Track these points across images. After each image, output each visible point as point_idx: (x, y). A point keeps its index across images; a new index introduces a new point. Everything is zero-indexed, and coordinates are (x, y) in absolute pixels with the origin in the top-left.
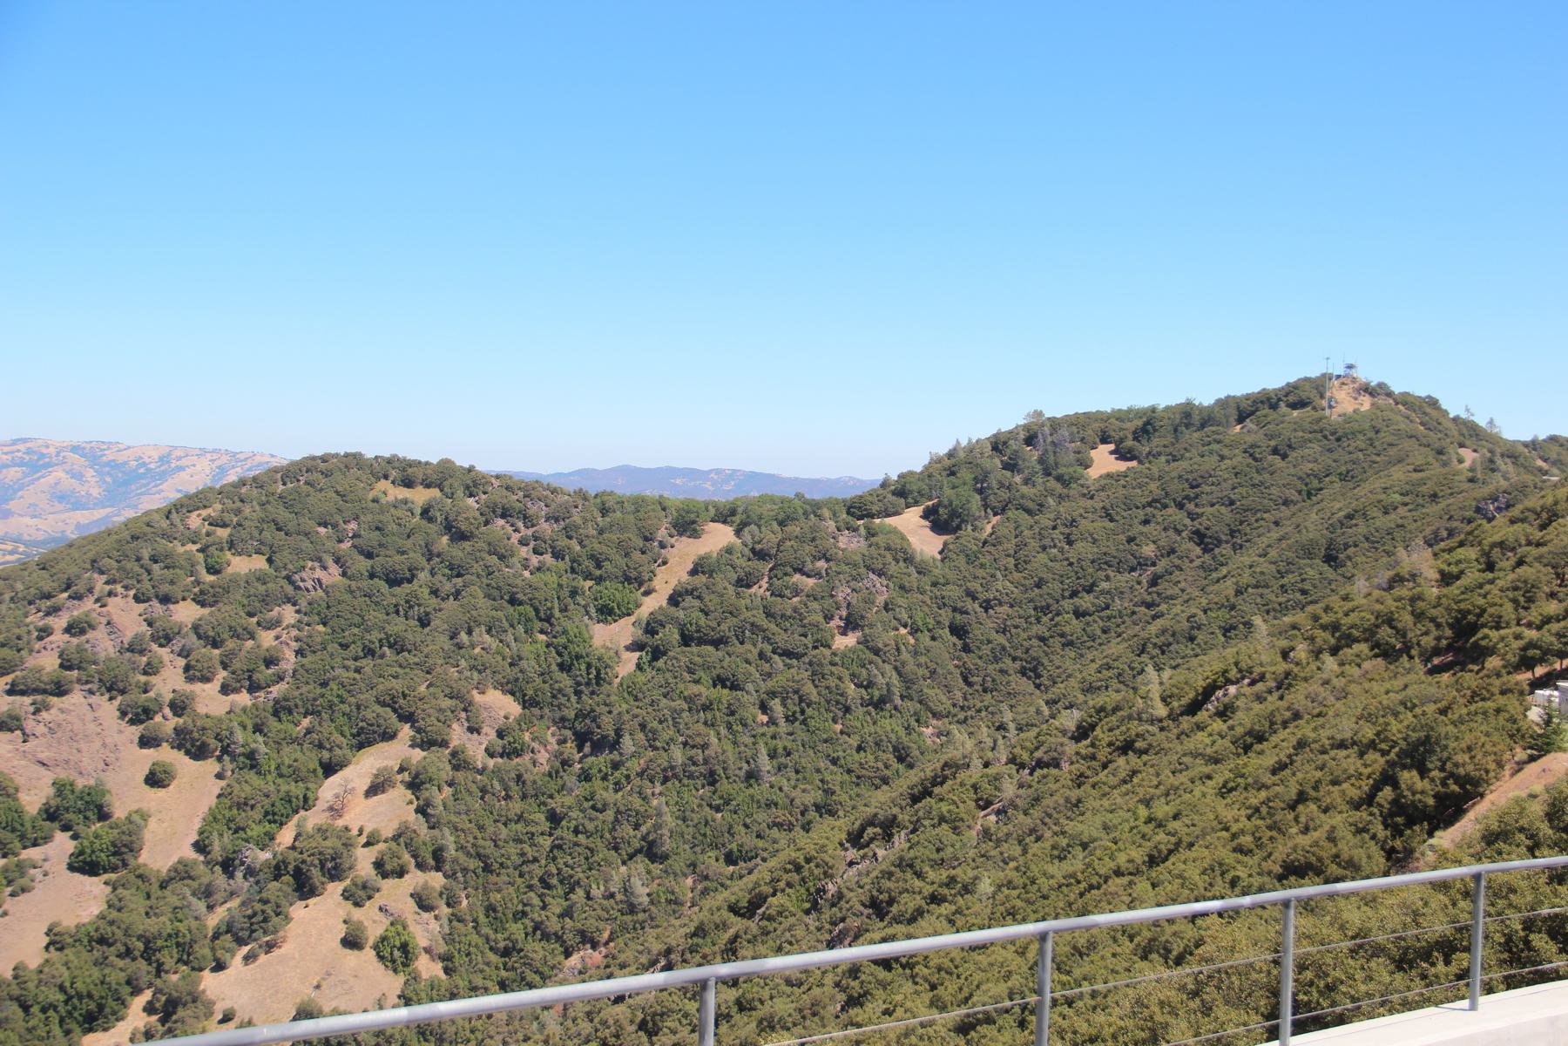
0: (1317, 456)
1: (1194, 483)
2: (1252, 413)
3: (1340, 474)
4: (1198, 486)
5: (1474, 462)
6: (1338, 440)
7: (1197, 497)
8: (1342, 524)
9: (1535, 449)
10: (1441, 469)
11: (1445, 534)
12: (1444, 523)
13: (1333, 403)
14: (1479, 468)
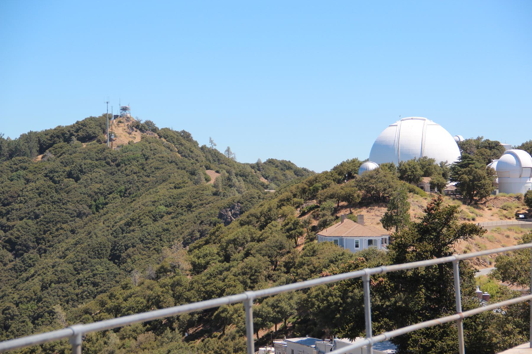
0: (103, 178)
1: (6, 202)
2: (51, 145)
3: (120, 192)
4: (8, 204)
5: (217, 180)
6: (118, 165)
7: (8, 213)
8: (123, 231)
9: (259, 170)
10: (194, 186)
11: (198, 235)
12: (197, 227)
13: (113, 137)
14: (220, 185)
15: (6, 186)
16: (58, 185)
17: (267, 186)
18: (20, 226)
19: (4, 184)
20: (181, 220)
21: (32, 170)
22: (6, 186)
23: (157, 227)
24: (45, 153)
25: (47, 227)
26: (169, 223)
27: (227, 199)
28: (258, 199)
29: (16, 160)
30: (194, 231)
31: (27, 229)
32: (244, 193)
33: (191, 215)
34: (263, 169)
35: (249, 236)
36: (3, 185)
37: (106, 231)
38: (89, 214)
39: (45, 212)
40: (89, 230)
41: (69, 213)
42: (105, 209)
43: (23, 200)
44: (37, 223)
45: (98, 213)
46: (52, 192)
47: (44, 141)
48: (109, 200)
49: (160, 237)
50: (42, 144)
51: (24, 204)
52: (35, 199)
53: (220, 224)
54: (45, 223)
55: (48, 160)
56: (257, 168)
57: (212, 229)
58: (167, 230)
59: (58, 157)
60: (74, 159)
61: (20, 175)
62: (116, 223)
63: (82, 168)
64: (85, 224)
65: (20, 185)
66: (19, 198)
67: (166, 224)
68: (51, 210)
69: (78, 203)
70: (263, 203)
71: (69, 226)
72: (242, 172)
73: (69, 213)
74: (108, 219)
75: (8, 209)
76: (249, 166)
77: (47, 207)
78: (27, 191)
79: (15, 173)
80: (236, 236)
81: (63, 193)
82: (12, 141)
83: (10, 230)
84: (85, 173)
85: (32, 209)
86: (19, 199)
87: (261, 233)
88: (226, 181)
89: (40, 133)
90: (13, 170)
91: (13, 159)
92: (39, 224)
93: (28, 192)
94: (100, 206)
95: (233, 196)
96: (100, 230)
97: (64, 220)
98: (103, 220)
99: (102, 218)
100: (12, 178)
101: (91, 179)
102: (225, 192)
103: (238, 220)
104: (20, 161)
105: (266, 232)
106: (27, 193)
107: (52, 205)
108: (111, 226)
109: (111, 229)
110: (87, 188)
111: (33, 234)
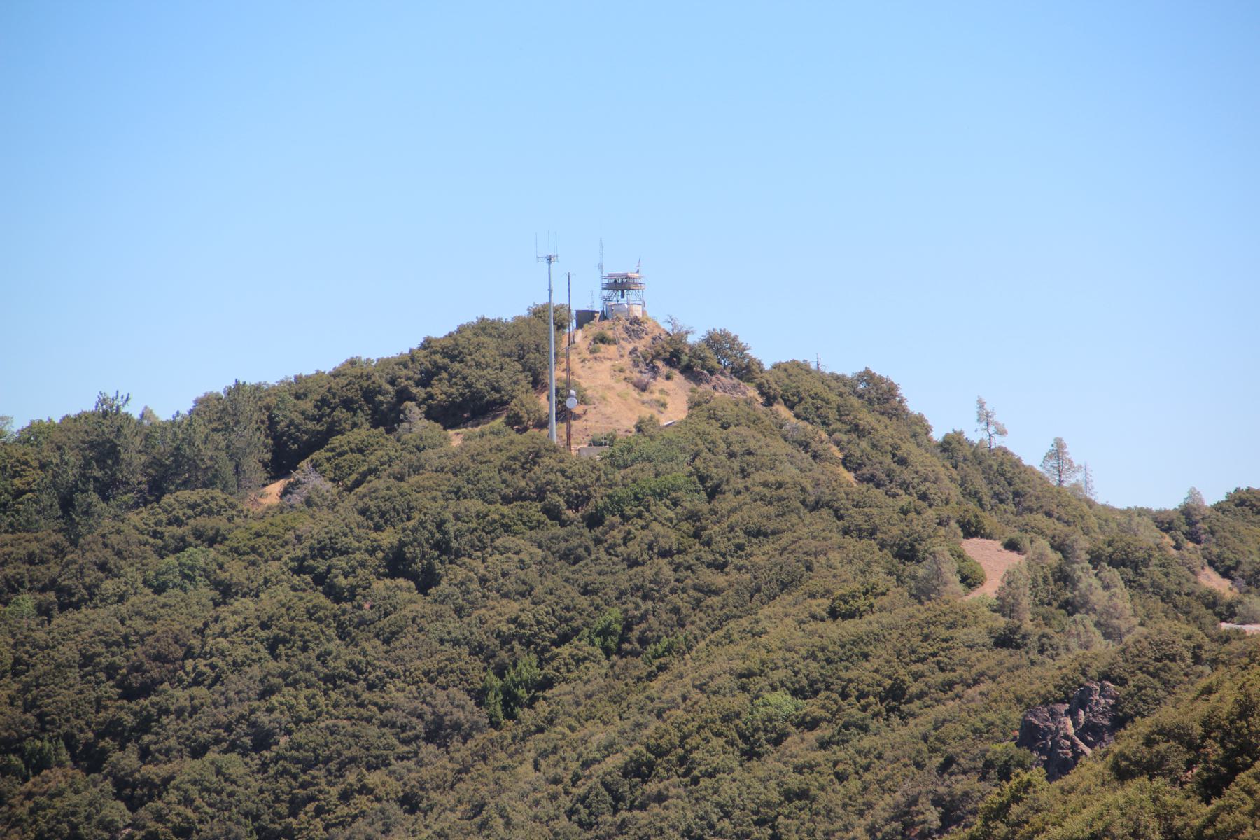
0: (532, 574)
1: (136, 680)
2: (319, 441)
3: (605, 632)
4: (147, 689)
5: (1010, 581)
6: (594, 521)
7: (145, 724)
8: (618, 798)
9: (1194, 537)
10: (912, 609)
11: (933, 816)
12: (926, 783)
13: (571, 403)
14: (1026, 602)
15: (139, 613)
16: (347, 606)
17: (1230, 606)
18: (194, 783)
19: (128, 604)
20: (859, 752)
21: (244, 545)
22: (139, 613)
23: (757, 785)
24: (296, 475)
25: (304, 786)
26: (811, 768)
27: (1058, 664)
28: (1189, 661)
29: (176, 505)
30: (914, 801)
31: (224, 796)
32: (1128, 639)
33: (904, 731)
34: (1213, 532)
35: (1154, 823)
36: (123, 609)
37: (544, 802)
38: (475, 727)
39: (298, 721)
40: (478, 796)
41: (393, 725)
42: (541, 706)
43: (207, 670)
44: (264, 767)
45: (511, 723)
46: (323, 638)
47: (292, 422)
48: (557, 670)
49: (773, 828)
50: (283, 434)
51: (210, 687)
52: (256, 667)
53: (1026, 770)
54: (294, 769)
55: (309, 502)
56: (1185, 528)
57: (993, 794)
58: (803, 794)
59: (350, 490)
60: (415, 495)
61: (192, 568)
62: (586, 765)
63: (446, 533)
64: (459, 772)
65: (195, 608)
66: (189, 664)
67: (798, 770)
68: (319, 714)
69: (431, 681)
70: (1213, 679)
71: (391, 781)
72: (1120, 545)
73: (393, 725)
74: (555, 750)
75: (144, 708)
76: (1147, 521)
77: (302, 701)
78: (224, 634)
79: (171, 560)
80: (1099, 825)
81: (368, 640)
82: (164, 427)
83: (151, 799)
84: (458, 554)
85: (243, 709)
86: (189, 669)
87: (1206, 810)
88: (1052, 587)
89: (274, 391)
90: (165, 547)
91: (167, 499)
92: (272, 771)
93: (226, 636)
94: (521, 692)
95: (1082, 651)
96: (523, 796)
97: (375, 752)
98: (533, 754)
99: (530, 745)
100: (163, 578)
101: (483, 581)
102: (1048, 631)
103: (1106, 755)
104: (192, 506)
105: (1229, 809)
106: (223, 643)
107: (326, 693)
108: (567, 780)
109: (567, 793)
110: (466, 620)
111: (246, 815)
